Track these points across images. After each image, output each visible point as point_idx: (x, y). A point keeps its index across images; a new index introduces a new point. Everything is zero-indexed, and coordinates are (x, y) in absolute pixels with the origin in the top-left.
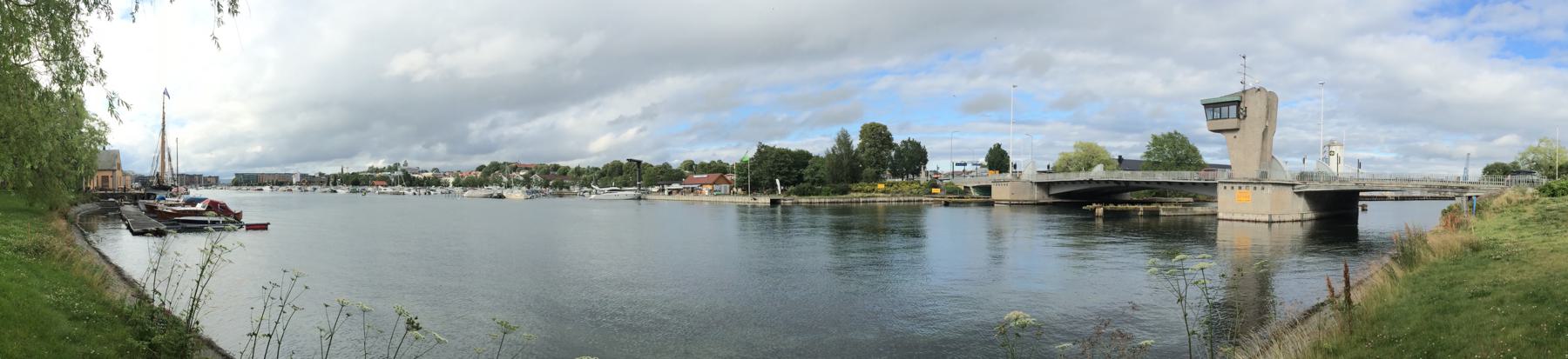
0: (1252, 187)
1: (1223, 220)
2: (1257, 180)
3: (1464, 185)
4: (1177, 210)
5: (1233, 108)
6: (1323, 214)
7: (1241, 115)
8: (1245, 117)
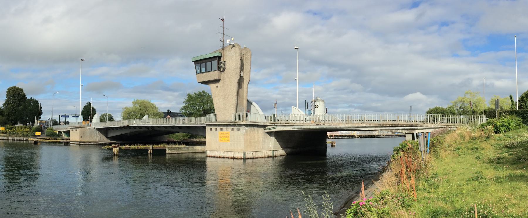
0: (230, 128)
1: (210, 157)
2: (233, 122)
3: (413, 123)
4: (181, 148)
5: (215, 63)
6: (289, 150)
7: (221, 69)
8: (224, 69)
